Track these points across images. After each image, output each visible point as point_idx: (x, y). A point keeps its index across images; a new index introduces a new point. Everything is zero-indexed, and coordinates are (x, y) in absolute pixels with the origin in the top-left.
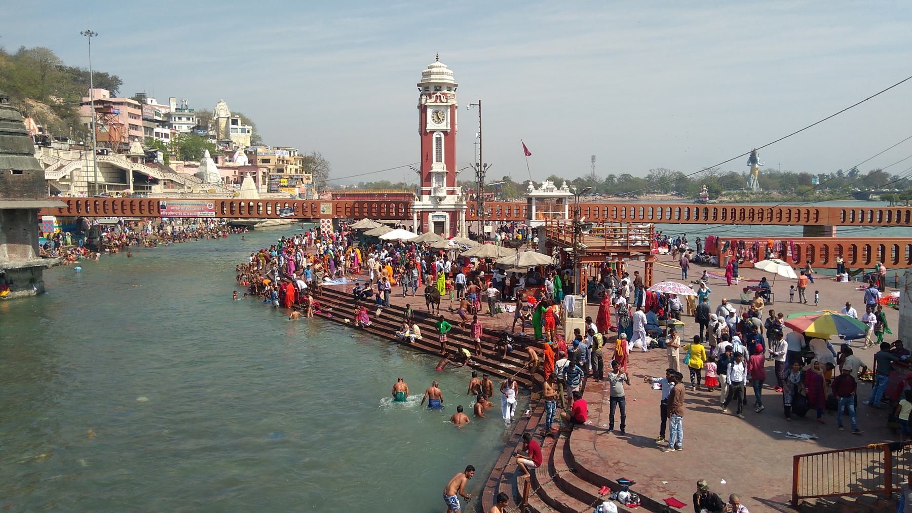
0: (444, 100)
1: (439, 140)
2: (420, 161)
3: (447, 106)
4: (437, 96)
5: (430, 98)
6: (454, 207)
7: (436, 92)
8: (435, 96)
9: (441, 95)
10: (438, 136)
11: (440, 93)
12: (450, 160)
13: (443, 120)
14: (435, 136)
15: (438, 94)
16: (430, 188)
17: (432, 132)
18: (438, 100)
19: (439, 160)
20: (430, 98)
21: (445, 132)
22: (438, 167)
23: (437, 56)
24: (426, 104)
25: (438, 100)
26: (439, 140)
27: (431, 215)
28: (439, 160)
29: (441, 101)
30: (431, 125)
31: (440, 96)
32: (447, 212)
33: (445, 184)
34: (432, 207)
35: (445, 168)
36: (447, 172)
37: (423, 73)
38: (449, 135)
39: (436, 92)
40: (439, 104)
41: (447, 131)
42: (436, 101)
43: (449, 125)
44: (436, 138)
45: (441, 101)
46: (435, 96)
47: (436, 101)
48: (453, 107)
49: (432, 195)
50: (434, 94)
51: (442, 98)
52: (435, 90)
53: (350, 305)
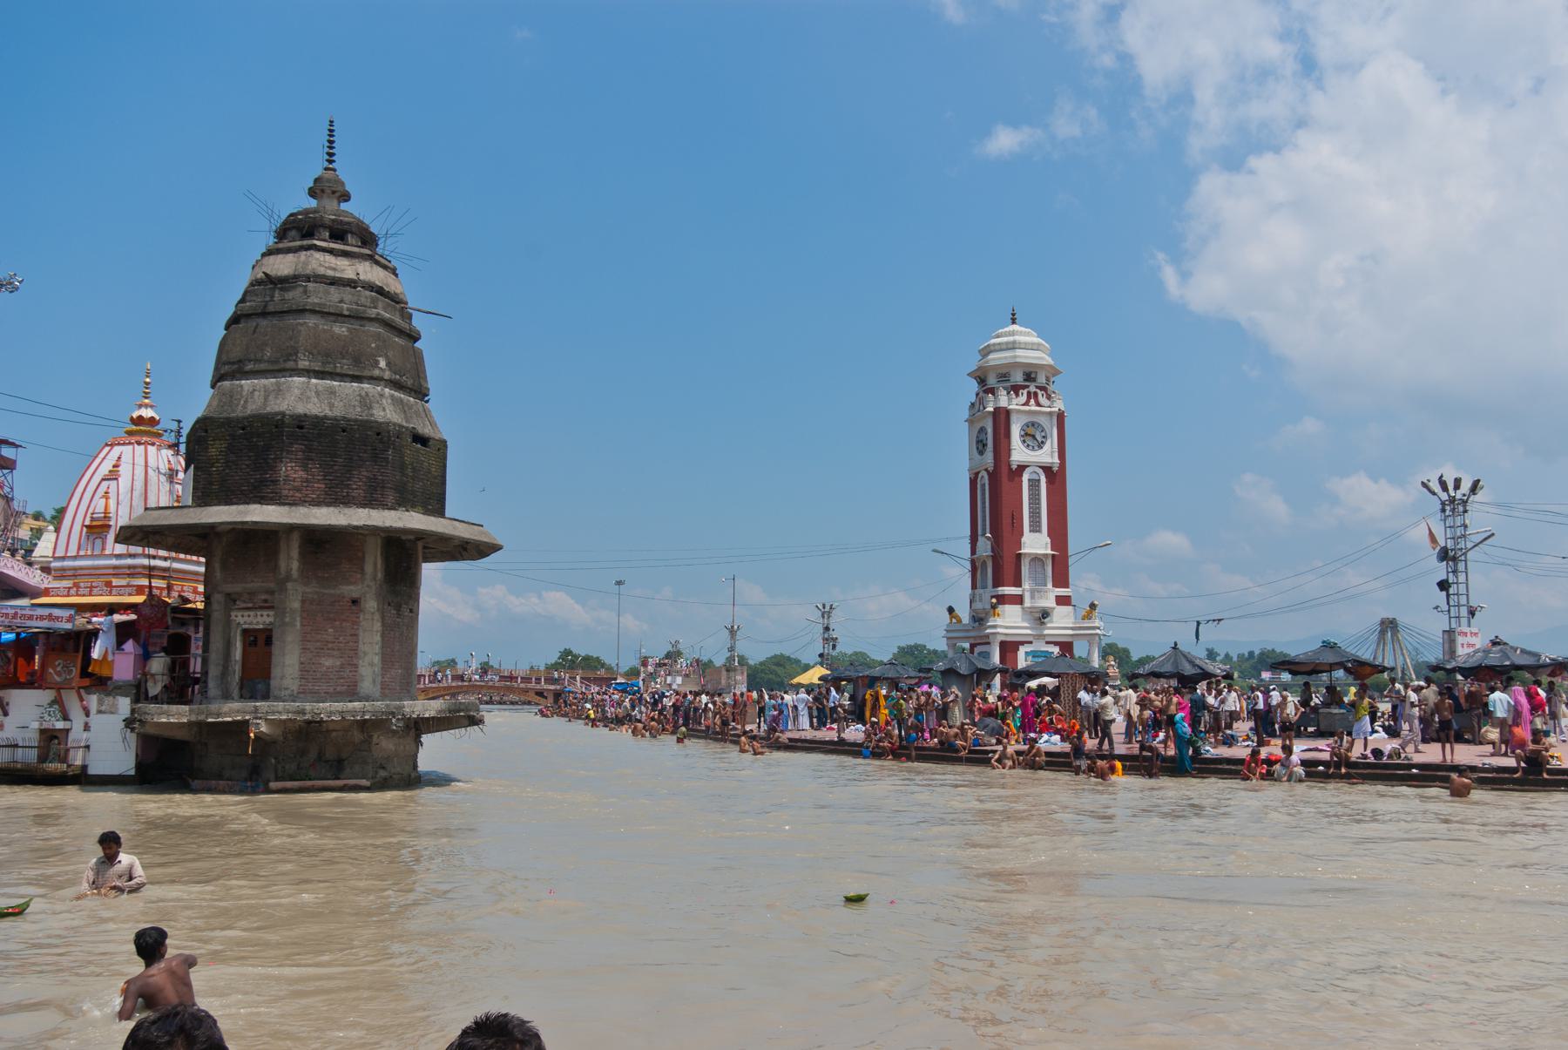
0: (1043, 400)
1: (1034, 484)
2: (968, 533)
3: (1050, 414)
4: (1029, 393)
5: (1017, 395)
6: (1071, 632)
7: (1027, 384)
8: (1025, 392)
9: (1038, 391)
10: (1036, 477)
11: (1037, 387)
13: (1042, 442)
14: (1025, 477)
15: (1032, 389)
16: (1020, 589)
17: (1022, 468)
18: (1032, 402)
20: (1017, 395)
21: (1047, 470)
22: (1035, 543)
23: (1013, 315)
24: (1011, 407)
25: (1032, 402)
26: (1034, 484)
27: (1022, 651)
28: (1035, 528)
29: (1038, 404)
30: (1019, 453)
31: (1036, 394)
32: (1056, 643)
33: (1050, 585)
34: (1029, 632)
35: (1049, 546)
36: (1053, 555)
37: (979, 351)
38: (1055, 477)
39: (1027, 384)
42: (1026, 404)
43: (1056, 455)
45: (1038, 404)
46: (1025, 392)
47: (1026, 404)
48: (1061, 417)
49: (1027, 603)
50: (1024, 387)
51: (1040, 396)
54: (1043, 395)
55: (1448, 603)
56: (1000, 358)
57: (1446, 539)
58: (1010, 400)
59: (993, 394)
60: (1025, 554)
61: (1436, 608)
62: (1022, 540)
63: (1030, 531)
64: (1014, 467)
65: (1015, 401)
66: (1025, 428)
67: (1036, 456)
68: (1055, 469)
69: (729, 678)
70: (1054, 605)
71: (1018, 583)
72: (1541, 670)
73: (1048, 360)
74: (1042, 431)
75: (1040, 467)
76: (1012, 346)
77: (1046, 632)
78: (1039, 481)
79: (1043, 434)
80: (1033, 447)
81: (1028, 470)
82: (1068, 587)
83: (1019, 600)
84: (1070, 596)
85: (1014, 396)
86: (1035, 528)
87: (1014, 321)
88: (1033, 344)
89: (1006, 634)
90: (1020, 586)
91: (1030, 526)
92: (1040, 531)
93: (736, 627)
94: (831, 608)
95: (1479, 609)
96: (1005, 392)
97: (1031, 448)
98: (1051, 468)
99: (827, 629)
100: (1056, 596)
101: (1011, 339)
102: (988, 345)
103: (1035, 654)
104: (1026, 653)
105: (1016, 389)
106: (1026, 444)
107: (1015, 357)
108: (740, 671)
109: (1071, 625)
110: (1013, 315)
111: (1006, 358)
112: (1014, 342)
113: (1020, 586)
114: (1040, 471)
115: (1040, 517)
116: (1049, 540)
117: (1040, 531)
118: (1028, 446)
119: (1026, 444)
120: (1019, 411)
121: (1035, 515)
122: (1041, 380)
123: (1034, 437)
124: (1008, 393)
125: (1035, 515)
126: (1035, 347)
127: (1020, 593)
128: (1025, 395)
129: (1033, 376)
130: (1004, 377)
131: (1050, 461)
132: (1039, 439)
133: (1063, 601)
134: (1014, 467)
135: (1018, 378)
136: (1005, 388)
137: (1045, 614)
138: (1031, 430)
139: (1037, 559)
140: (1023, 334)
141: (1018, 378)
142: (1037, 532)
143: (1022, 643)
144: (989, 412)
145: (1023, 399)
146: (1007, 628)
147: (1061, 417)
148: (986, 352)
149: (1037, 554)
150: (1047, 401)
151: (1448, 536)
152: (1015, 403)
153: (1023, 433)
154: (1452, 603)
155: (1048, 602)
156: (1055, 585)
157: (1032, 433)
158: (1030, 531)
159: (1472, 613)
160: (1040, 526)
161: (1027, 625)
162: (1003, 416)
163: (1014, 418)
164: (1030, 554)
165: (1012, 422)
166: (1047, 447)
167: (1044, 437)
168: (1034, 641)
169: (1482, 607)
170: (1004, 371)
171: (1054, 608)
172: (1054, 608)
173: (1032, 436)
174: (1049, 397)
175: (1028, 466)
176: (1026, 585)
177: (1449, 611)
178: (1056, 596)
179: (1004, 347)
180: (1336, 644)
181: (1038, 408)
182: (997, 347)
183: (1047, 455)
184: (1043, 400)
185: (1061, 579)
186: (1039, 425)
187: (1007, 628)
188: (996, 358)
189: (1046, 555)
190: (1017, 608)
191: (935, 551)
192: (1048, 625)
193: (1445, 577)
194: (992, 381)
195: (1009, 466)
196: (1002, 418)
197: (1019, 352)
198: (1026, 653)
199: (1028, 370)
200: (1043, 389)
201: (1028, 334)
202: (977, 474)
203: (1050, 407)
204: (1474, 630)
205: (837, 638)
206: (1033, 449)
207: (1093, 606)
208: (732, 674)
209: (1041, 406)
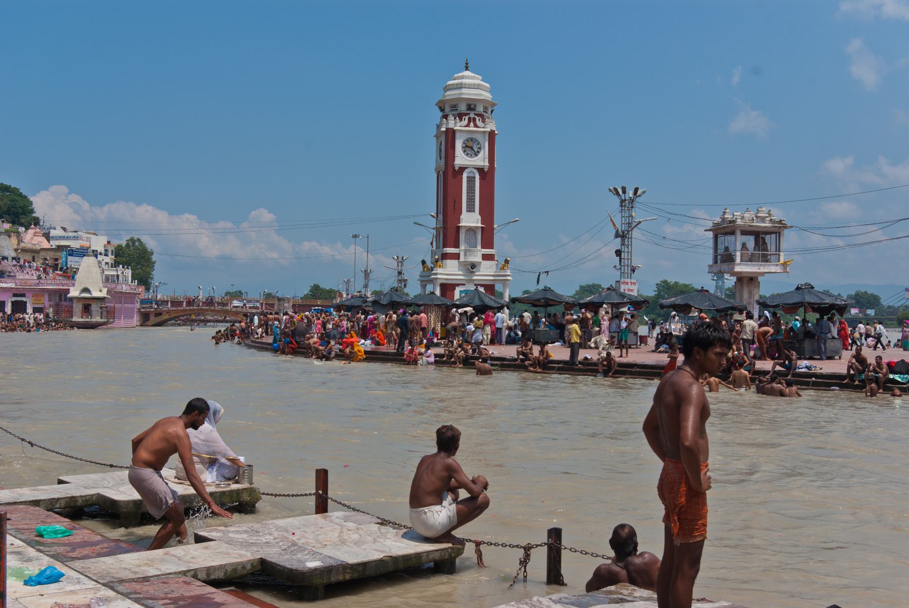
0: (479, 123)
1: (471, 180)
3: (484, 132)
4: (469, 119)
5: (461, 120)
6: (492, 278)
8: (467, 118)
9: (476, 117)
10: (472, 175)
11: (475, 114)
12: (487, 213)
13: (478, 152)
14: (465, 175)
15: (472, 116)
16: (459, 249)
17: (462, 169)
18: (472, 124)
20: (461, 120)
21: (480, 170)
22: (470, 219)
23: (467, 64)
24: (455, 128)
25: (472, 124)
26: (471, 180)
27: (457, 291)
28: (471, 209)
29: (476, 126)
30: (461, 159)
31: (474, 119)
33: (479, 247)
34: (462, 277)
35: (480, 221)
36: (482, 227)
38: (487, 175)
40: (472, 128)
41: (483, 169)
42: (468, 125)
43: (487, 160)
45: (476, 126)
46: (467, 118)
47: (468, 125)
48: (492, 135)
49: (462, 259)
50: (466, 114)
52: (468, 110)
53: (639, 370)
54: (479, 120)
55: (620, 264)
56: (452, 95)
57: (622, 224)
58: (455, 123)
59: (446, 119)
60: (462, 226)
61: (615, 267)
62: (462, 217)
63: (467, 211)
64: (457, 168)
65: (459, 124)
66: (466, 142)
67: (472, 161)
68: (486, 170)
69: (279, 305)
70: (481, 260)
71: (457, 245)
72: (621, 305)
73: (487, 96)
74: (478, 144)
75: (475, 168)
76: (460, 86)
77: (475, 278)
78: (474, 177)
79: (479, 146)
80: (471, 155)
81: (467, 170)
82: (493, 249)
83: (456, 257)
84: (494, 255)
85: (458, 121)
86: (471, 209)
87: (467, 69)
88: (474, 85)
89: (447, 279)
90: (459, 247)
91: (467, 208)
92: (474, 211)
93: (369, 271)
94: (402, 259)
95: (637, 268)
96: (453, 118)
97: (469, 155)
98: (483, 169)
99: (400, 273)
100: (483, 255)
101: (460, 81)
102: (446, 86)
103: (466, 292)
104: (461, 291)
105: (460, 116)
106: (466, 153)
107: (461, 94)
108: (286, 301)
109: (493, 274)
110: (467, 64)
111: (455, 94)
112: (461, 84)
113: (459, 247)
114: (476, 171)
115: (474, 202)
116: (479, 217)
117: (474, 211)
118: (468, 154)
119: (466, 153)
120: (461, 131)
121: (471, 200)
122: (480, 109)
123: (472, 148)
124: (455, 118)
125: (471, 200)
126: (476, 87)
127: (458, 252)
128: (467, 120)
129: (472, 107)
130: (454, 107)
131: (483, 164)
132: (476, 149)
133: (486, 257)
134: (457, 168)
135: (463, 108)
136: (453, 115)
137: (473, 266)
138: (470, 144)
139: (471, 230)
140: (469, 77)
141: (463, 108)
142: (472, 211)
143: (458, 285)
144: (443, 131)
145: (465, 122)
146: (447, 275)
147: (492, 135)
148: (447, 88)
149: (470, 226)
150: (482, 124)
151: (623, 222)
152: (458, 125)
153: (464, 145)
154: (623, 264)
155: (477, 258)
157: (471, 146)
158: (467, 211)
159: (633, 270)
160: (474, 208)
161: (461, 273)
162: (450, 134)
163: (458, 135)
164: (465, 227)
165: (456, 138)
166: (481, 155)
167: (479, 148)
168: (466, 284)
169: (639, 267)
170: (454, 103)
171: (481, 262)
172: (481, 262)
173: (471, 148)
174: (484, 121)
175: (467, 168)
176: (462, 247)
177: (620, 269)
178: (483, 255)
179: (455, 87)
180: (550, 288)
181: (475, 129)
182: (451, 87)
183: (481, 160)
184: (479, 123)
185: (488, 242)
186: (476, 140)
187: (447, 275)
188: (451, 94)
189: (477, 227)
190: (456, 261)
191: (415, 223)
192: (477, 273)
193: (619, 248)
194: (447, 110)
195: (454, 167)
196: (451, 135)
197: (464, 91)
198: (461, 291)
199: (470, 102)
200: (479, 115)
201: (473, 78)
202: (439, 172)
203: (484, 128)
204: (633, 281)
205: (406, 279)
206: (471, 156)
207: (507, 262)
208: (282, 302)
209: (479, 127)
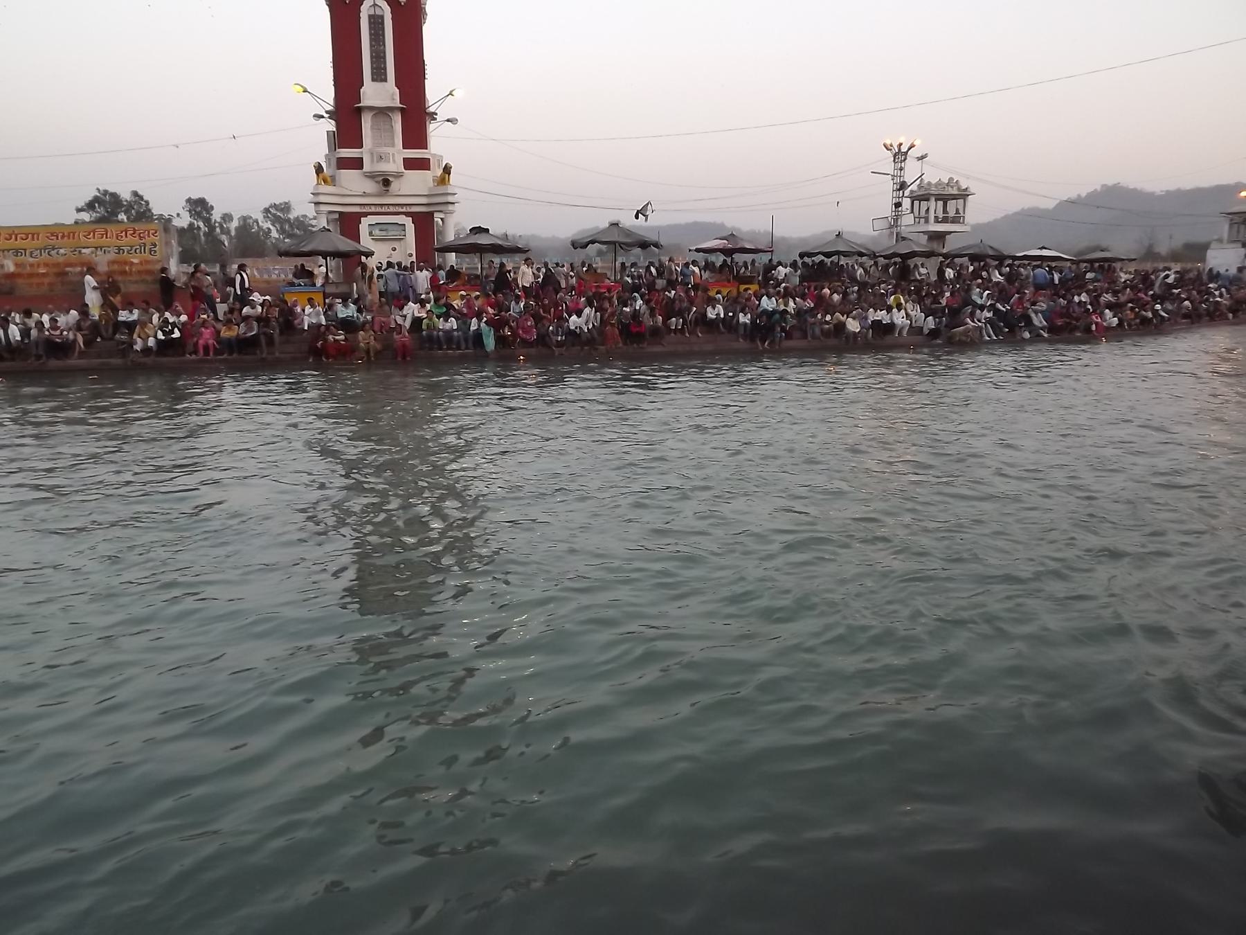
1: (376, 23)
6: (424, 200)
19: (379, 75)
36: (402, 110)
44: (370, 17)
49: (367, 166)
62: (362, 90)
63: (373, 80)
78: (382, 17)
83: (357, 164)
86: (379, 75)
91: (373, 74)
92: (385, 80)
109: (426, 194)
117: (385, 80)
121: (378, 58)
125: (378, 58)
133: (410, 164)
143: (366, 215)
155: (394, 165)
156: (406, 145)
158: (373, 80)
